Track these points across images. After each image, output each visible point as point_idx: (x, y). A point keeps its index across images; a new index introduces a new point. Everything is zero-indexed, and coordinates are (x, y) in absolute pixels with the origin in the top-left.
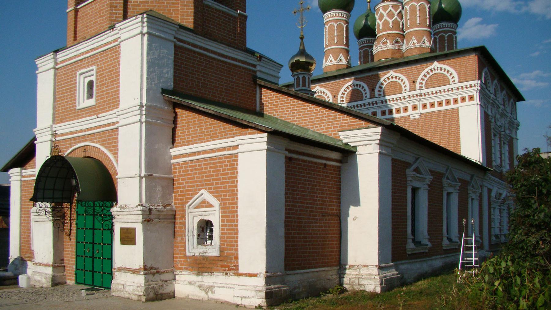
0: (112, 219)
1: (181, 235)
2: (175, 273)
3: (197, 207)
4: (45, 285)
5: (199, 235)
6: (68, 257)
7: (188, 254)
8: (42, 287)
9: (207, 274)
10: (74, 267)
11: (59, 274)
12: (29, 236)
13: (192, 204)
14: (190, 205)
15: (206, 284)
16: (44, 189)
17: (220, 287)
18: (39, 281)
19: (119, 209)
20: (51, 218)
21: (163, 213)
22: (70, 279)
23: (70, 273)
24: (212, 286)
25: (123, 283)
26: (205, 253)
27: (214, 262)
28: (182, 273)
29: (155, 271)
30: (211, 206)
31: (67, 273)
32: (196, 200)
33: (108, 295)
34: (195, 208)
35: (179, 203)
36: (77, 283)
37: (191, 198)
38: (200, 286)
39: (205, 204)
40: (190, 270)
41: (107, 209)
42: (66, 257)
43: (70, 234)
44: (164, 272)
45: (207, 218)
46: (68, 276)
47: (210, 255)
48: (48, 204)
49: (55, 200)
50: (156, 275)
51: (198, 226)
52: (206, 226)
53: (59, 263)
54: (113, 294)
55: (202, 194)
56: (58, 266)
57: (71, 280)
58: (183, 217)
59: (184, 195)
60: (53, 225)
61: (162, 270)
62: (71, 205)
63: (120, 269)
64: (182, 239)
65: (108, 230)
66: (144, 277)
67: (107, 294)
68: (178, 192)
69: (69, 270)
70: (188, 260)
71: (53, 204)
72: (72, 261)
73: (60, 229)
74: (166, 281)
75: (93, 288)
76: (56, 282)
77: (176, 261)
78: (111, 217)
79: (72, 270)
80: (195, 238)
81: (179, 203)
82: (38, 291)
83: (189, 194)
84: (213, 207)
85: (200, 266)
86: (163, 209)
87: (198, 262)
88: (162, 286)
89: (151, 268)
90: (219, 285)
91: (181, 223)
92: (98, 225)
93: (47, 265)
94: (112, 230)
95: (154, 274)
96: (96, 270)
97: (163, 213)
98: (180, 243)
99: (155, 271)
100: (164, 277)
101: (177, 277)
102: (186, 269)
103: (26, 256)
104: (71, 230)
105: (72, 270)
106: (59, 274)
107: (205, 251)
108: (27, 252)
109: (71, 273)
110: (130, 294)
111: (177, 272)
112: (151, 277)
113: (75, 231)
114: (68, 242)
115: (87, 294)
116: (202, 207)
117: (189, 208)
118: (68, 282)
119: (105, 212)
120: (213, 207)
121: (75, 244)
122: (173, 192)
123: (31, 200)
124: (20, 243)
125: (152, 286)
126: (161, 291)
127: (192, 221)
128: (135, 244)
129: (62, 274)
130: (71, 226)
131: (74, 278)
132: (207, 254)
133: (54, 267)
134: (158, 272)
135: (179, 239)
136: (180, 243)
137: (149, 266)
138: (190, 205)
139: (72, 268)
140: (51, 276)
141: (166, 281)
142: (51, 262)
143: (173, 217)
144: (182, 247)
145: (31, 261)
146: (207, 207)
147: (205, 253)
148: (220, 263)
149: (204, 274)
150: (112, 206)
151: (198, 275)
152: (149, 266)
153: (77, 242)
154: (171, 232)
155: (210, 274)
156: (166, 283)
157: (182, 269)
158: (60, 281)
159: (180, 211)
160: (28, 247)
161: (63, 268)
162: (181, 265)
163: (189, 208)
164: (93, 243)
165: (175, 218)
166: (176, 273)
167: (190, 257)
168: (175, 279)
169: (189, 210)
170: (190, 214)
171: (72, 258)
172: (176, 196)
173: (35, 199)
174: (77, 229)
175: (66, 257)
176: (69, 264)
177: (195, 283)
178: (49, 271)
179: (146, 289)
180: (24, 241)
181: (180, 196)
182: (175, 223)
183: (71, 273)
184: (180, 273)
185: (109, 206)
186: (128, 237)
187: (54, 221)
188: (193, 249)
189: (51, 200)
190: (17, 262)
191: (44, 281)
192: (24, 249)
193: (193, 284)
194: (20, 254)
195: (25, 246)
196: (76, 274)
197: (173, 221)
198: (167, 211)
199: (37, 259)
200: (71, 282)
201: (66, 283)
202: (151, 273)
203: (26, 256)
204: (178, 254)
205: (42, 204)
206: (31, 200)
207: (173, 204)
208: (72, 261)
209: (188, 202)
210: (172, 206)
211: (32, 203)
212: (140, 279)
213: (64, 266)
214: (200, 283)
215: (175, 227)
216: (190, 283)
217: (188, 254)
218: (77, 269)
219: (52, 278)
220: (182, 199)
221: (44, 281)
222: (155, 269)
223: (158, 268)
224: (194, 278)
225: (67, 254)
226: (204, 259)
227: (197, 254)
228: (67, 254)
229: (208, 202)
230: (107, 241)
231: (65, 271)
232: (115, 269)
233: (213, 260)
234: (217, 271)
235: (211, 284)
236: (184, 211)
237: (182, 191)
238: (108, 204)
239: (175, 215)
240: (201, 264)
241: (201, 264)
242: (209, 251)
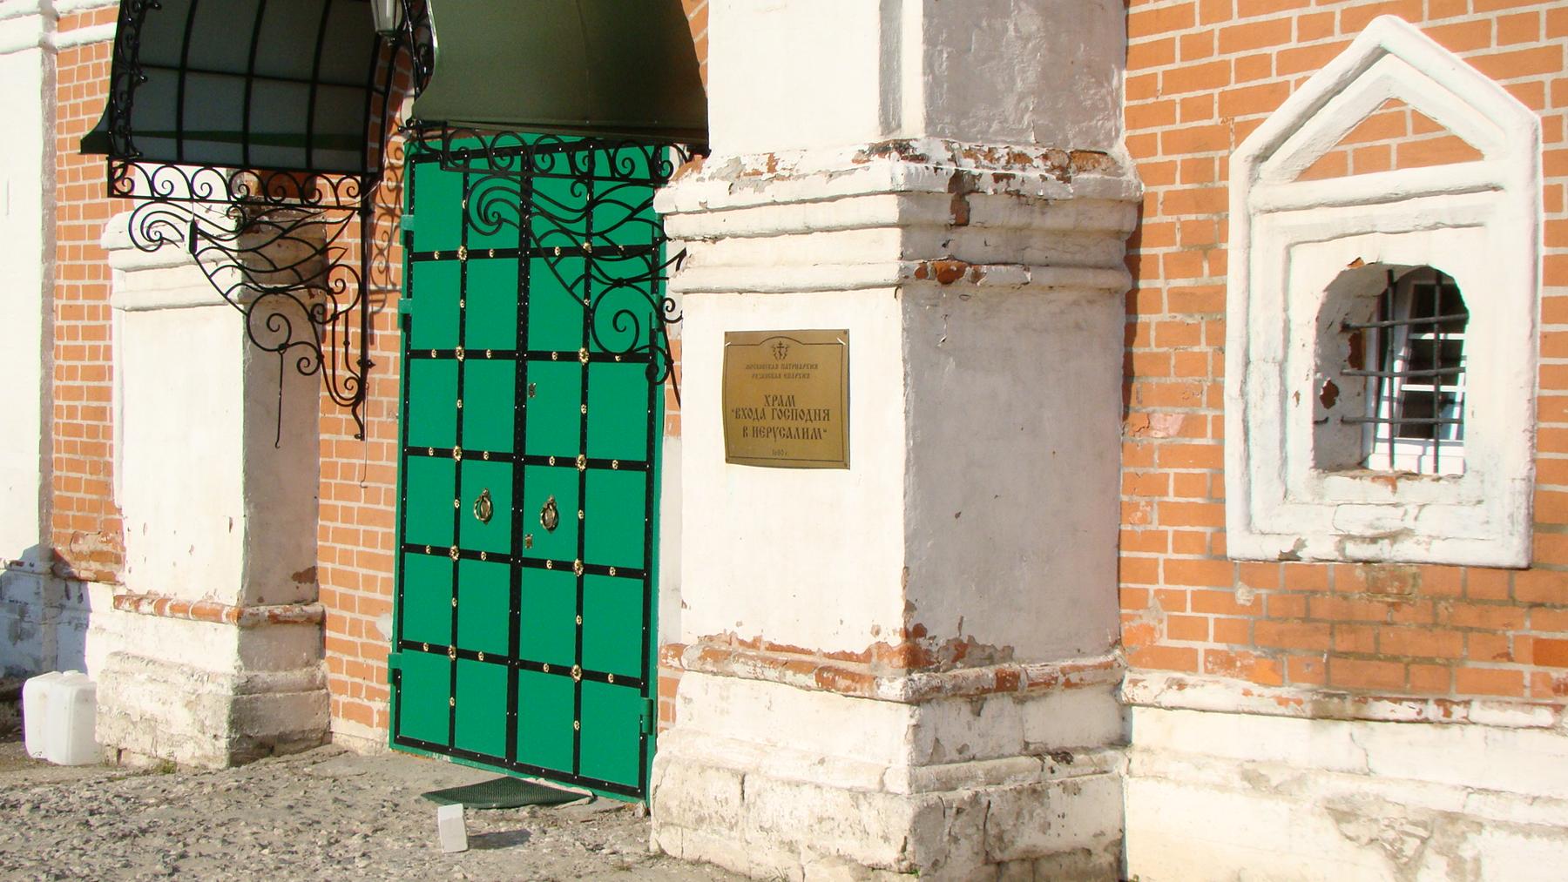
0: (655, 274)
1: (1184, 396)
2: (1127, 691)
3: (1326, 166)
4: (186, 755)
5: (1328, 396)
6: (346, 557)
7: (1239, 545)
8: (168, 768)
9: (1406, 710)
10: (386, 625)
11: (281, 676)
12: (101, 414)
13: (1284, 136)
14: (1263, 156)
15: (1395, 793)
16: (183, 69)
17: (1528, 830)
18: (150, 723)
19: (716, 193)
20: (231, 278)
21: (1054, 221)
22: (351, 713)
23: (354, 669)
24: (1451, 818)
25: (740, 760)
26: (1394, 537)
27: (1468, 616)
28: (1189, 696)
29: (989, 672)
30: (1458, 150)
31: (336, 665)
32: (1321, 105)
33: (630, 853)
34: (1306, 174)
35: (1173, 143)
36: (400, 740)
37: (1277, 95)
38: (1342, 814)
39: (1401, 136)
40: (1249, 673)
41: (634, 195)
42: (330, 555)
43: (361, 396)
44: (1048, 683)
45: (1405, 254)
46: (341, 687)
47: (1439, 553)
48: (212, 181)
49: (259, 153)
50: (993, 705)
51: (1324, 323)
52: (1401, 330)
53: (281, 602)
54: (662, 838)
55: (1380, 53)
56: (274, 619)
57: (364, 716)
58: (1206, 247)
59: (1217, 75)
60: (249, 332)
61: (1035, 670)
62: (369, 180)
63: (718, 654)
64: (1192, 425)
65: (630, 356)
66: (905, 717)
67: (615, 838)
68: (1161, 53)
69: (349, 648)
70: (1243, 595)
71: (250, 179)
72: (370, 583)
73: (292, 355)
74: (1064, 756)
75: (517, 783)
76: (263, 737)
77: (1140, 601)
78: (652, 256)
79: (368, 650)
80: (1303, 413)
81: (1173, 143)
82: (134, 802)
83: (1262, 66)
84: (1473, 154)
85: (1343, 643)
86: (1054, 189)
87: (1323, 607)
88: (1037, 793)
89: (961, 651)
90: (1521, 813)
91: (1182, 300)
92: (554, 323)
93: (205, 613)
94: (655, 360)
95: (976, 698)
96: (537, 650)
97: (1054, 221)
98: (1172, 455)
99: (989, 672)
100: (1054, 720)
101: (1143, 725)
102: (1224, 663)
103: (83, 546)
104: (365, 364)
105: (368, 650)
106: (281, 676)
107: (1392, 520)
108: (87, 524)
109: (366, 673)
110: (791, 847)
111: (1147, 685)
112: (954, 721)
113: (394, 376)
114: (343, 450)
115: (479, 841)
116: (1372, 162)
117: (1253, 178)
118: (345, 731)
119: (604, 216)
120: (1473, 154)
121: (395, 465)
122: (1126, 56)
123: (90, 145)
124: (46, 466)
125: (964, 793)
126: (1028, 838)
127: (1278, 274)
128: (840, 460)
129: (299, 675)
130: (366, 340)
131: (382, 706)
132: (1407, 551)
133: (248, 623)
134: (1006, 684)
135: (1164, 424)
136: (1172, 455)
137: (942, 632)
138: (1263, 156)
139: (373, 632)
140: (227, 692)
141: (1064, 756)
142: (230, 591)
143: (1117, 251)
144: (1184, 485)
145: (111, 579)
146: (1412, 157)
147: (1394, 537)
148: (1529, 629)
149: (1382, 709)
150: (658, 177)
151: (1322, 715)
152: (942, 632)
153: (409, 452)
154: (1105, 371)
155: (1432, 711)
156: (1063, 771)
157: (1187, 661)
158: (291, 725)
159: (1175, 203)
160: (91, 487)
161: (312, 632)
162: (1180, 628)
163: (1253, 178)
164: (520, 459)
165: (1132, 264)
166: (1139, 694)
167: (1253, 569)
168: (1122, 742)
169: (1259, 196)
170: (1260, 222)
171: (370, 561)
172: (1140, 87)
173: (116, 140)
174: (412, 354)
175: (330, 555)
176: (347, 603)
177: (1300, 780)
178: (218, 652)
179: (926, 820)
180: (71, 447)
181: (1176, 81)
182: (1131, 302)
183: (366, 673)
184: (1172, 697)
185: (642, 172)
186: (790, 406)
187: (259, 300)
188: (1285, 501)
189: (234, 151)
190: (23, 590)
191: (181, 720)
192: (67, 503)
193: (1277, 790)
194: (44, 531)
195: (73, 485)
196: (396, 677)
197: (1121, 280)
198: (1081, 198)
199: (135, 578)
200: (361, 731)
201: (326, 736)
202: (957, 691)
203: (83, 546)
204: (1157, 541)
205: (171, 178)
206: (90, 145)
207: (1119, 150)
208: (370, 583)
209: (1245, 130)
210: (1115, 167)
211: (100, 161)
212: (876, 737)
213: (321, 622)
214: (1345, 786)
215: (1130, 332)
216: (1254, 779)
217: (1239, 545)
218: (403, 644)
219: (236, 705)
220: (1197, 109)
221: (181, 720)
222: (991, 660)
223: (1008, 653)
224: (1292, 740)
225: (341, 536)
226: (1375, 588)
227: (1319, 547)
228: (341, 536)
229: (1424, 123)
230: (616, 438)
231: (321, 653)
232: (678, 649)
233: (1464, 598)
234: (1503, 690)
235: (1451, 802)
236: (1215, 201)
237: (1198, 46)
238: (634, 158)
239: (1134, 240)
240: (1349, 624)
241: (1349, 624)
242: (1428, 523)
